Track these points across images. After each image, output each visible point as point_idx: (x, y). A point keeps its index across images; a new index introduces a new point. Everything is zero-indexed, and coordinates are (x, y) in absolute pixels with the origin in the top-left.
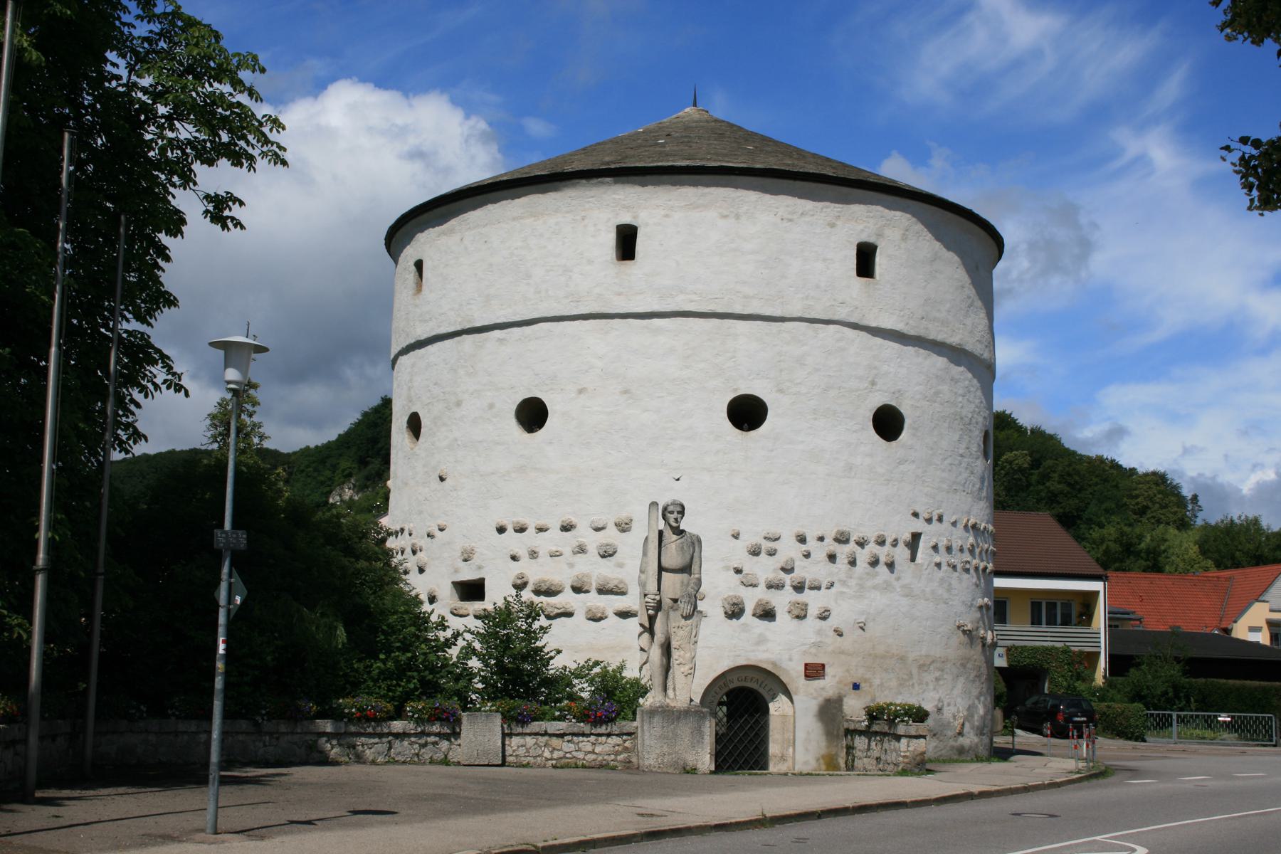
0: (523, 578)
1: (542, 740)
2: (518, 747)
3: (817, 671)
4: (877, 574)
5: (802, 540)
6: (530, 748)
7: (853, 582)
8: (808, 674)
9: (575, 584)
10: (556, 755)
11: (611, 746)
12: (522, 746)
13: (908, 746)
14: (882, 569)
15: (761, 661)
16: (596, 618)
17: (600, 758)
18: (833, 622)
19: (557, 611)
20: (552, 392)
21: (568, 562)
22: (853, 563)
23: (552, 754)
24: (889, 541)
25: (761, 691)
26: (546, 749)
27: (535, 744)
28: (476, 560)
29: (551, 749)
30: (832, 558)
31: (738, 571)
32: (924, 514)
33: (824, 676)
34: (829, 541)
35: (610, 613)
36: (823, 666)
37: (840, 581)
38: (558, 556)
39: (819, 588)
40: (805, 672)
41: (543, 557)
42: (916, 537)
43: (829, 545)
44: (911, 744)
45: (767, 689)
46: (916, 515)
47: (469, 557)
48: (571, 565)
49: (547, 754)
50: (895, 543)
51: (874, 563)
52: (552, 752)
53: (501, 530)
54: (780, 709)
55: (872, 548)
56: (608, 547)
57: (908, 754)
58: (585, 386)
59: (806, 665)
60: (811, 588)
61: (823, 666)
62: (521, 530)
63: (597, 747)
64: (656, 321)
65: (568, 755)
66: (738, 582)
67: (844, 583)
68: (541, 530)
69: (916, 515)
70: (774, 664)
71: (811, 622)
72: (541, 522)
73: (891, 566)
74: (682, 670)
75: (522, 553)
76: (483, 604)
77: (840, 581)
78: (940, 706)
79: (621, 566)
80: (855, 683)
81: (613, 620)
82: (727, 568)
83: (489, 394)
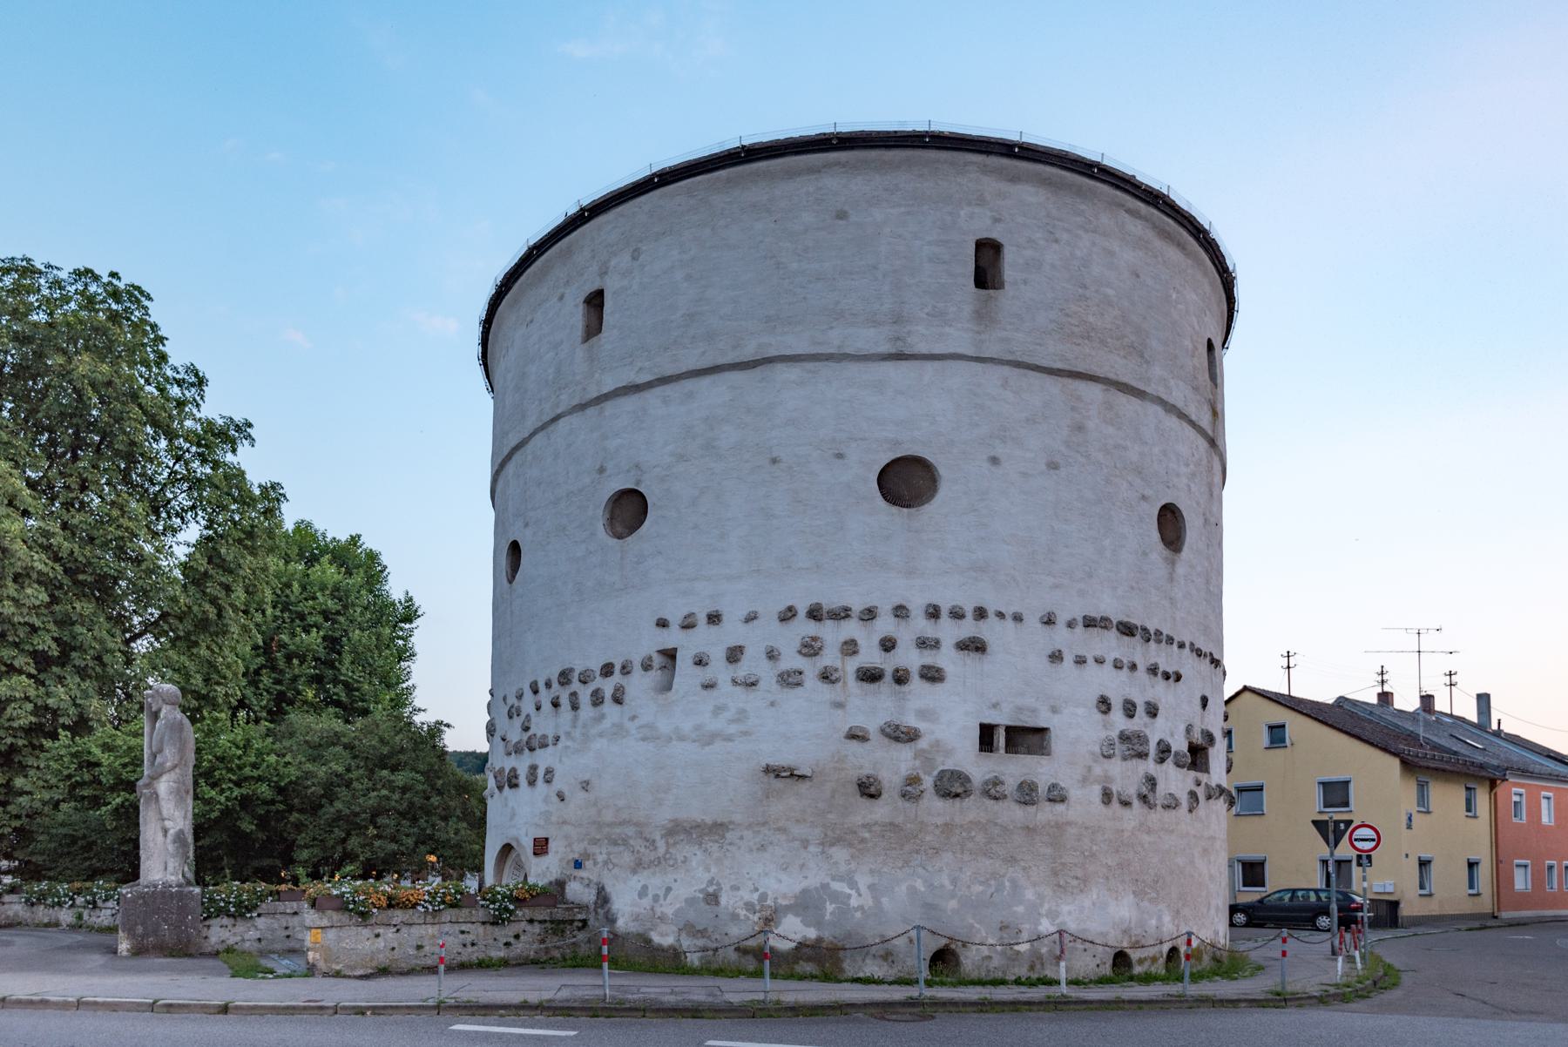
4: (602, 717)
14: (609, 707)
18: (558, 784)
32: (675, 618)
36: (547, 839)
39: (544, 746)
42: (670, 655)
46: (662, 624)
50: (626, 670)
61: (547, 839)
69: (662, 624)
78: (711, 890)
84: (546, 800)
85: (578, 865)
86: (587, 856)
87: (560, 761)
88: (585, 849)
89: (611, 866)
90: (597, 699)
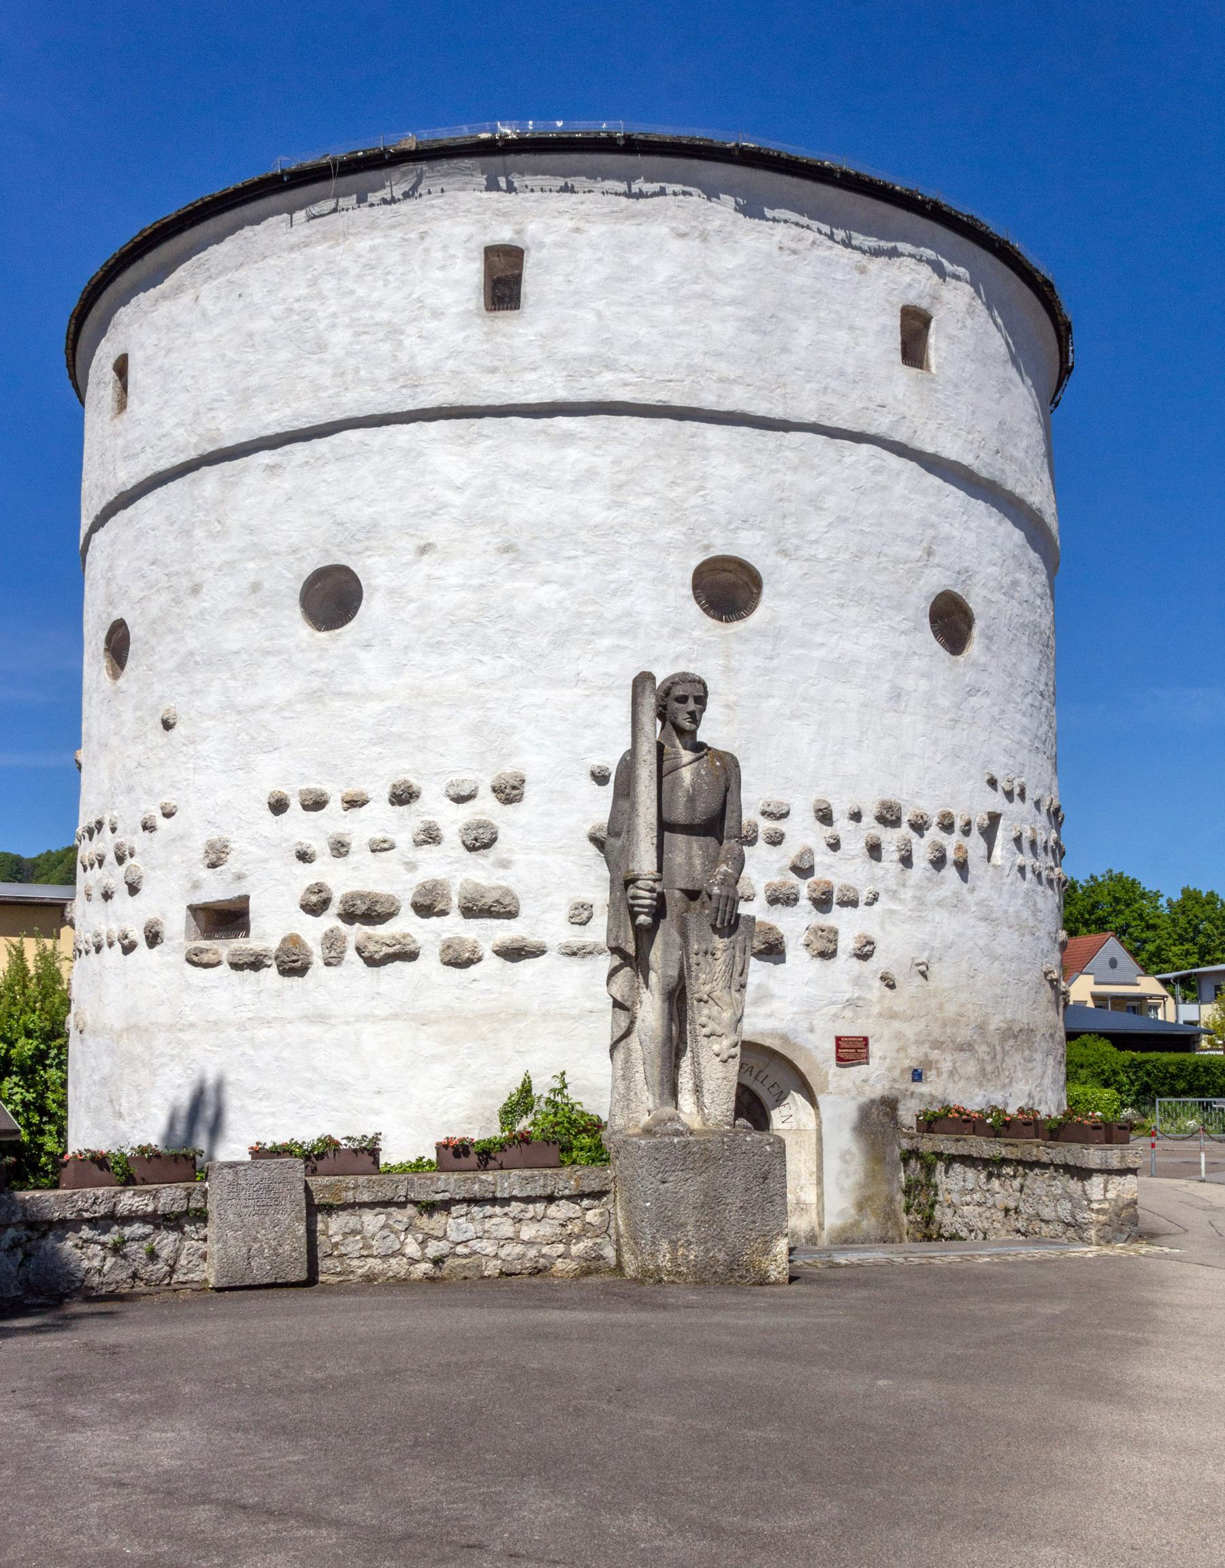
0: (320, 891)
1: (400, 1218)
2: (345, 1235)
4: (942, 882)
5: (825, 816)
6: (373, 1237)
7: (908, 894)
9: (420, 899)
10: (433, 1249)
11: (557, 1222)
12: (354, 1232)
13: (1106, 1190)
15: (762, 1034)
16: (460, 959)
17: (532, 1253)
18: (878, 963)
19: (386, 950)
20: (370, 553)
21: (407, 860)
22: (906, 861)
23: (423, 1249)
24: (959, 824)
26: (410, 1239)
27: (383, 1228)
28: (232, 864)
29: (420, 1237)
30: (874, 850)
33: (867, 1058)
34: (868, 819)
35: (486, 950)
36: (866, 1039)
37: (887, 891)
38: (386, 850)
39: (854, 903)
41: (359, 853)
42: (994, 818)
44: (1110, 1186)
45: (768, 1083)
47: (219, 859)
48: (411, 866)
49: (412, 1249)
51: (938, 862)
52: (423, 1244)
53: (278, 806)
54: (791, 1119)
55: (934, 833)
56: (481, 831)
57: (1106, 1206)
58: (431, 541)
59: (838, 1039)
60: (843, 904)
61: (866, 1039)
62: (316, 804)
64: (563, 422)
65: (460, 1250)
67: (894, 895)
68: (353, 803)
70: (784, 1038)
71: (844, 963)
72: (353, 789)
73: (962, 867)
74: (716, 1048)
75: (320, 847)
76: (248, 942)
77: (887, 891)
79: (504, 864)
80: (916, 1070)
81: (491, 964)
83: (251, 565)
84: (857, 981)
85: (917, 1076)
86: (929, 1064)
88: (926, 1055)
89: (957, 1078)
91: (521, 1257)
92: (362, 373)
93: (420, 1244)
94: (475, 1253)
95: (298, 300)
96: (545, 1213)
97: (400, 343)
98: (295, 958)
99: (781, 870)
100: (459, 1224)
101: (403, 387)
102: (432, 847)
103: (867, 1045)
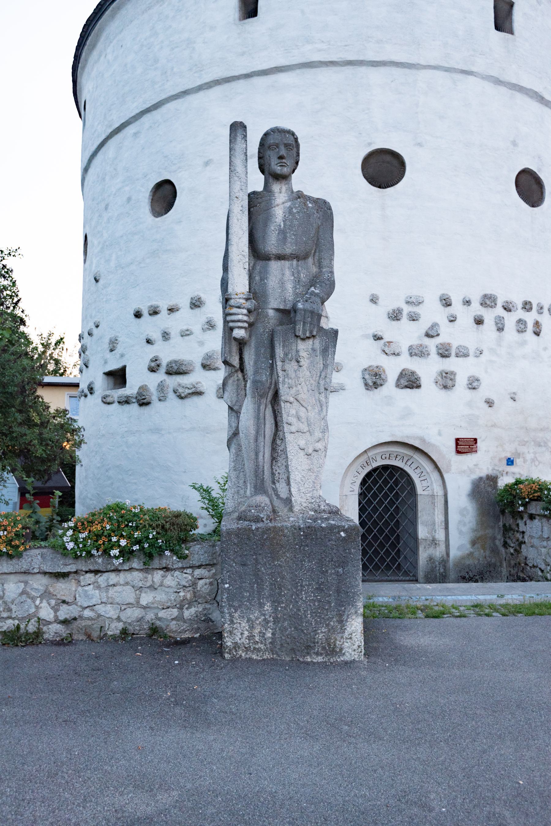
0: (156, 360)
3: (469, 446)
4: (523, 343)
5: (446, 302)
8: (460, 450)
9: (204, 362)
15: (407, 437)
18: (484, 392)
19: (188, 391)
20: (180, 170)
21: (199, 340)
25: (407, 469)
26: (44, 604)
28: (119, 349)
29: (53, 602)
30: (479, 321)
31: (378, 338)
36: (475, 440)
38: (188, 335)
39: (466, 355)
40: (457, 448)
41: (175, 338)
43: (476, 309)
47: (114, 347)
48: (201, 343)
53: (138, 315)
55: (520, 314)
58: (211, 158)
59: (457, 440)
61: (475, 440)
62: (154, 312)
63: (143, 595)
64: (282, 78)
65: (87, 613)
66: (379, 352)
67: (492, 351)
68: (171, 310)
70: (423, 440)
72: (171, 303)
75: (156, 336)
76: (125, 390)
80: (509, 459)
82: (366, 336)
84: (470, 404)
85: (510, 462)
86: (518, 455)
87: (486, 372)
88: (516, 449)
89: (537, 463)
90: (521, 326)
91: (140, 620)
92: (175, 70)
93: (52, 608)
94: (99, 616)
95: (146, 39)
96: (162, 582)
97: (194, 49)
98: (143, 397)
99: (419, 338)
100: (86, 591)
101: (195, 73)
102: (211, 332)
103: (476, 443)
